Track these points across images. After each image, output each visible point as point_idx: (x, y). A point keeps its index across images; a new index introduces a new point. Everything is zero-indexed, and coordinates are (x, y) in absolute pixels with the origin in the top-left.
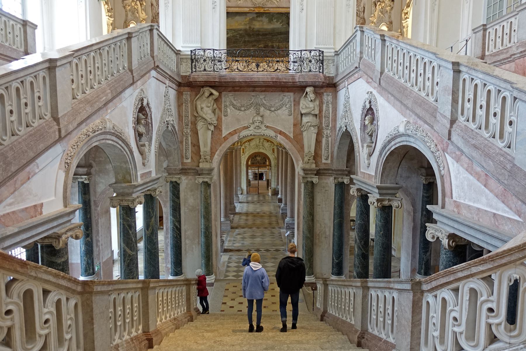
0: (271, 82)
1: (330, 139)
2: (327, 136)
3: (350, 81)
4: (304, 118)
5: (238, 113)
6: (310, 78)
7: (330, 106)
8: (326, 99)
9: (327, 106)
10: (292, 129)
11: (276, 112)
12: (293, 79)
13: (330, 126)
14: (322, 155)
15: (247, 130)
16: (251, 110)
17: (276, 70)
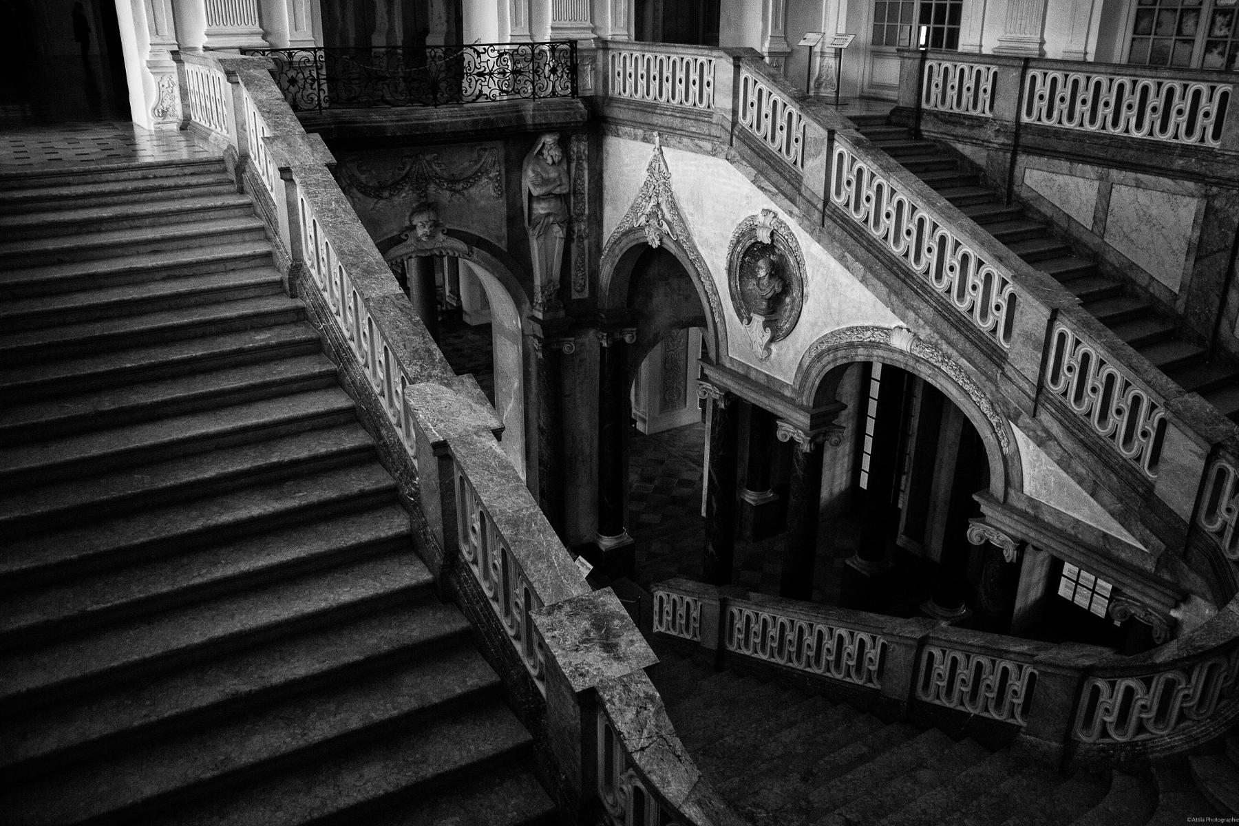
0: (472, 131)
1: (586, 242)
2: (580, 237)
3: (673, 141)
4: (535, 205)
5: (372, 206)
6: (558, 114)
7: (585, 165)
8: (575, 149)
9: (579, 165)
10: (504, 230)
11: (465, 192)
12: (521, 118)
13: (587, 212)
14: (570, 284)
15: (401, 246)
16: (404, 195)
17: (478, 97)
